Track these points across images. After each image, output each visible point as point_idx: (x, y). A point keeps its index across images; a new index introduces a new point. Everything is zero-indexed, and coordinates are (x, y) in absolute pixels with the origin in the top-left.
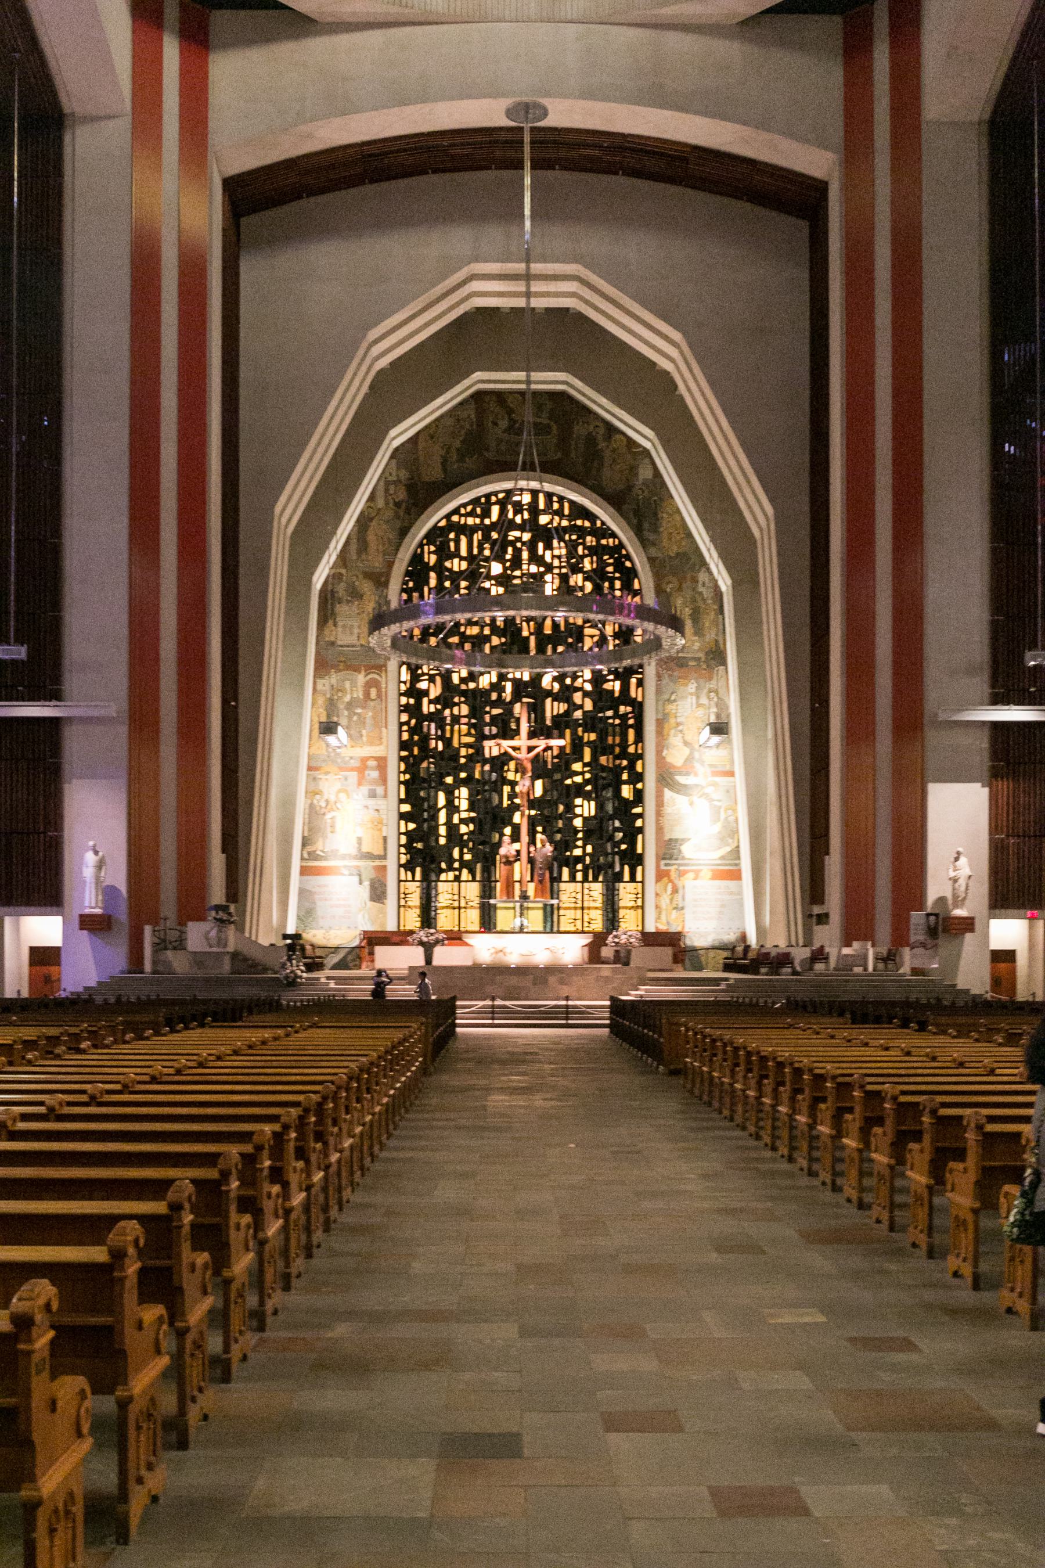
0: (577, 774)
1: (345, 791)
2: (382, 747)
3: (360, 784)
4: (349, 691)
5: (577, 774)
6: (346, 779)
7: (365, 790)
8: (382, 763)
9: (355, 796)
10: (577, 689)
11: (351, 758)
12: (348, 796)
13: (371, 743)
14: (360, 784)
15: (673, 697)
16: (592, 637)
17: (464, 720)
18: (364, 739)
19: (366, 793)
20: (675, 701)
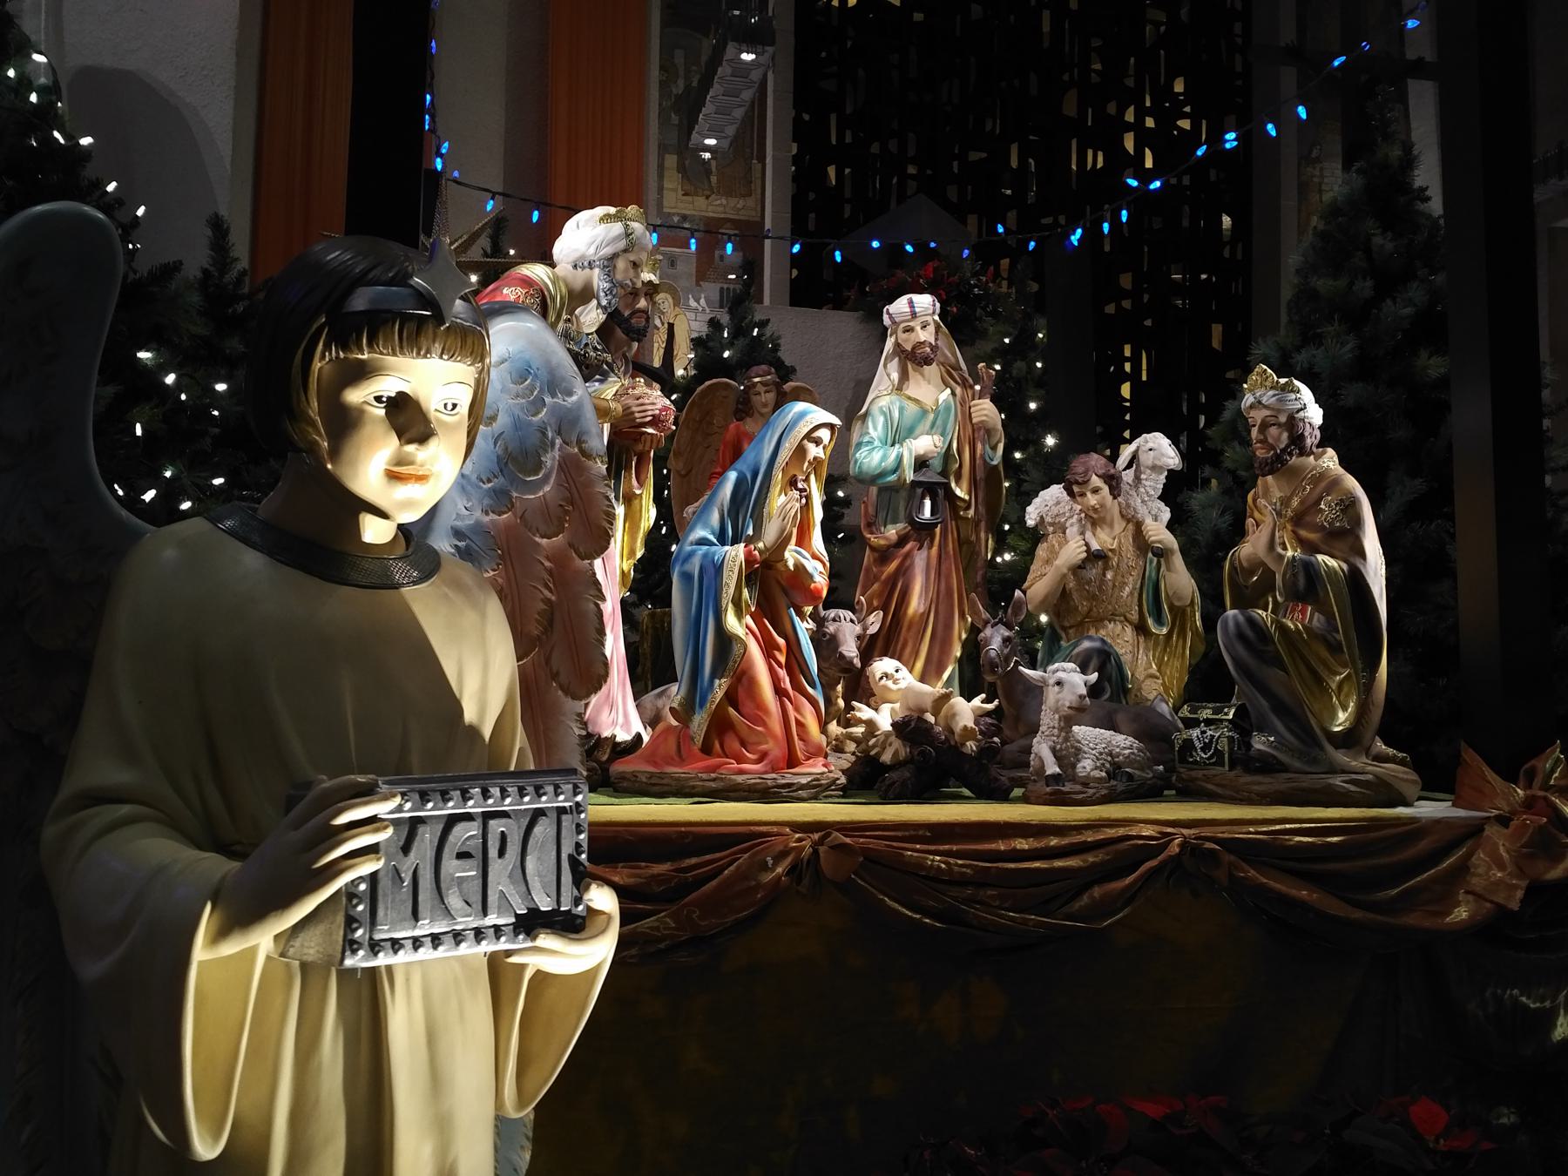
0: (1125, 294)
1: (673, 292)
2: (751, 202)
3: (701, 277)
4: (681, 73)
5: (1125, 294)
6: (673, 264)
7: (712, 289)
8: (750, 235)
9: (693, 303)
10: (1128, 127)
11: (684, 218)
12: (677, 303)
13: (729, 193)
14: (701, 277)
15: (1314, 154)
16: (1157, 24)
17: (912, 170)
18: (714, 179)
19: (716, 297)
20: (1318, 160)
